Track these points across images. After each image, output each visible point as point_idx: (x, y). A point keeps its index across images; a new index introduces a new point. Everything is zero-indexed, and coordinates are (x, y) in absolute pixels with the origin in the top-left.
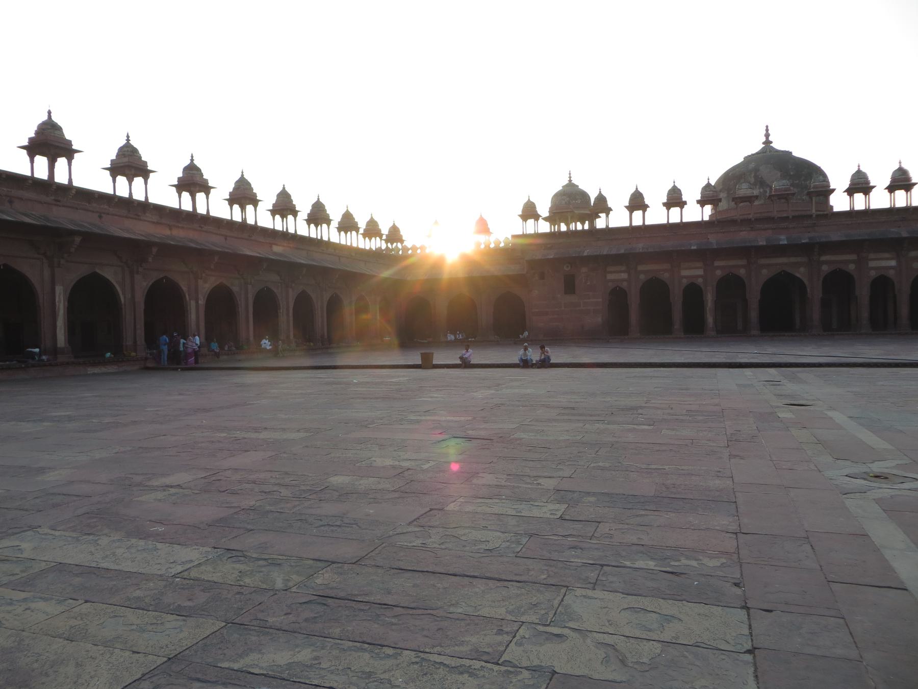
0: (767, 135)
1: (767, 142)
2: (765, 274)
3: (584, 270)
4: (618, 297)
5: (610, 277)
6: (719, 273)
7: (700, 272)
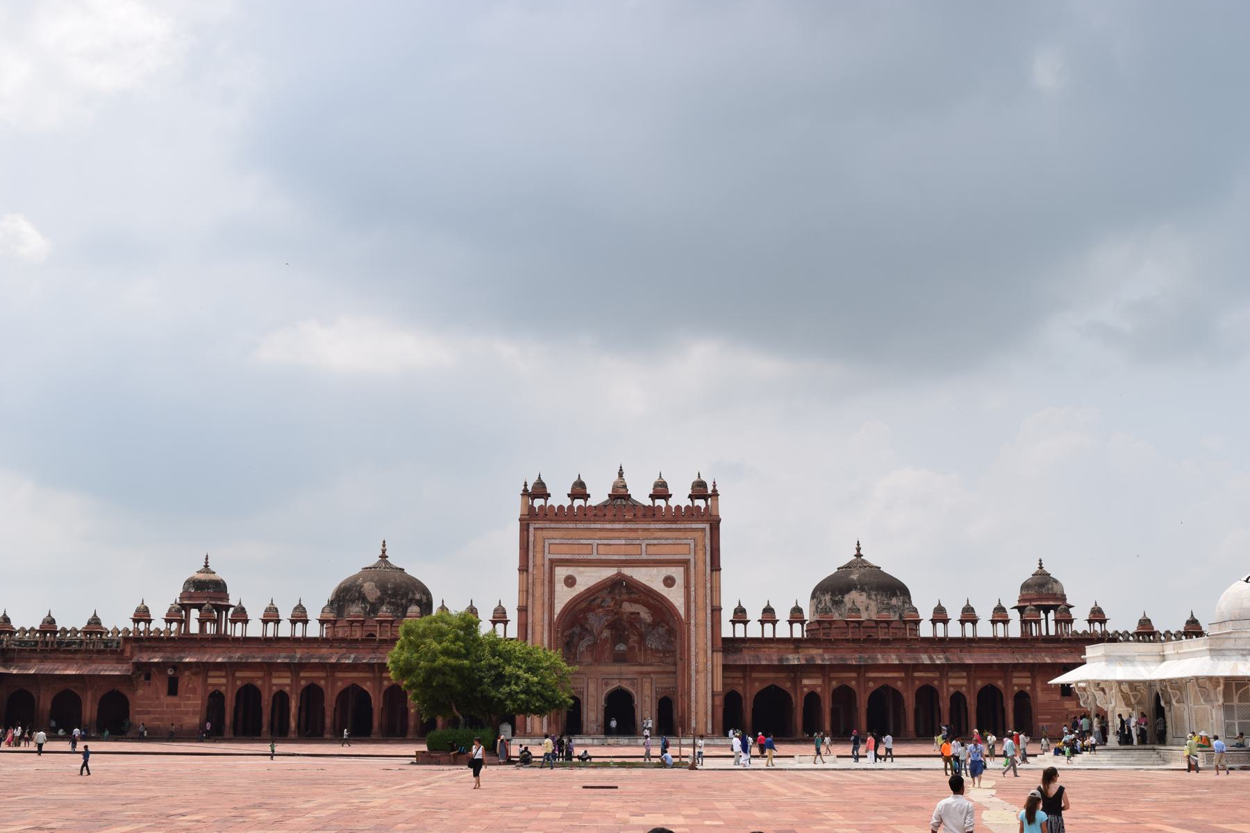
0: (384, 552)
1: (384, 556)
2: (340, 685)
3: (187, 673)
4: (216, 699)
5: (210, 681)
6: (303, 683)
7: (288, 681)
